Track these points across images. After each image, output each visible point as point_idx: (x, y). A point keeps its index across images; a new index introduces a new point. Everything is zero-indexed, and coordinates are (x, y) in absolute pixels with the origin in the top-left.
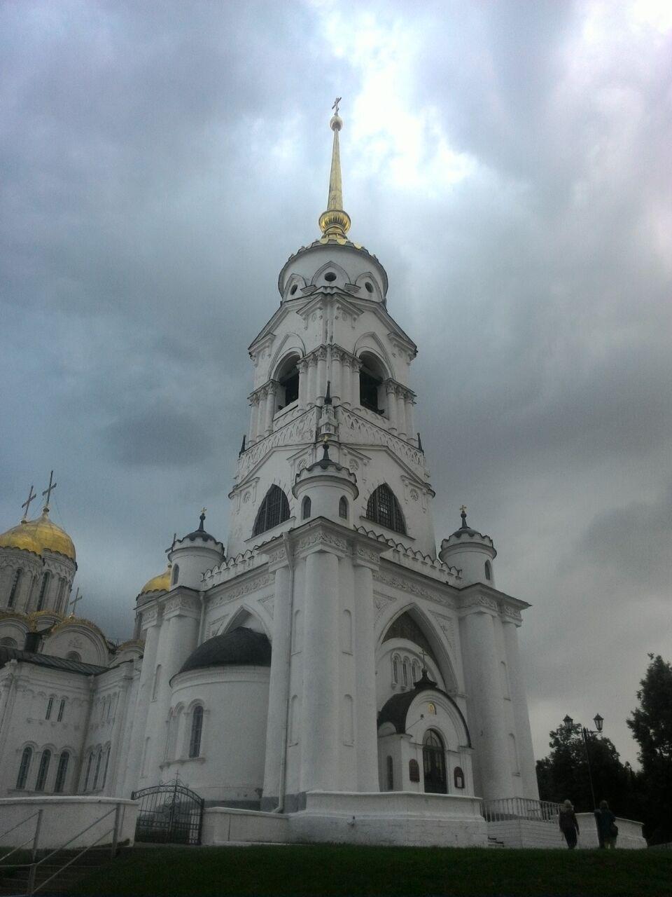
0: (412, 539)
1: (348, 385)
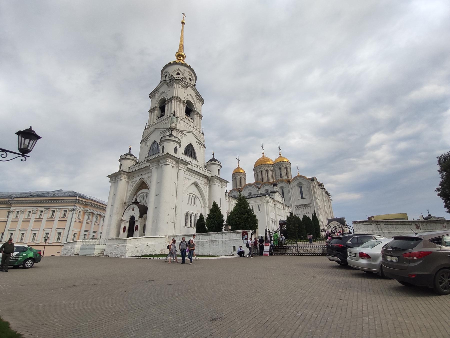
0: (198, 161)
1: (181, 110)
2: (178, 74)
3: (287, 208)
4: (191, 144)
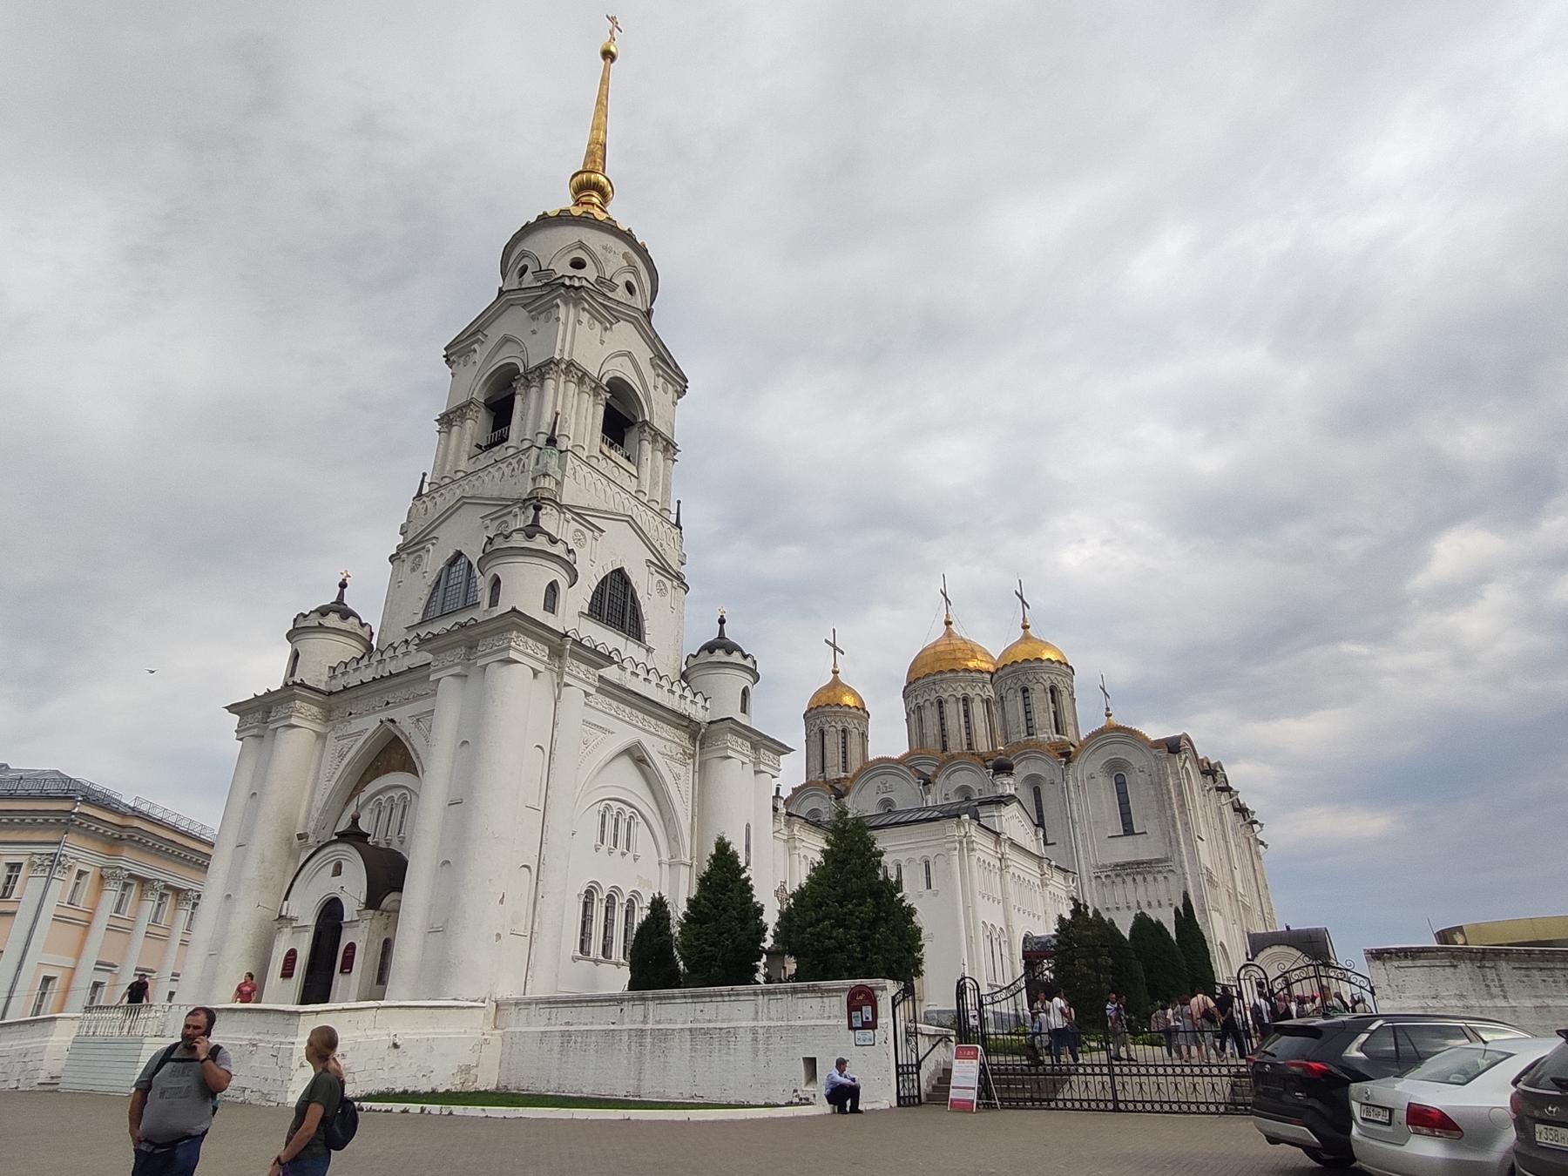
0: (649, 650)
1: (583, 419)
2: (578, 264)
3: (1058, 878)
4: (620, 572)
